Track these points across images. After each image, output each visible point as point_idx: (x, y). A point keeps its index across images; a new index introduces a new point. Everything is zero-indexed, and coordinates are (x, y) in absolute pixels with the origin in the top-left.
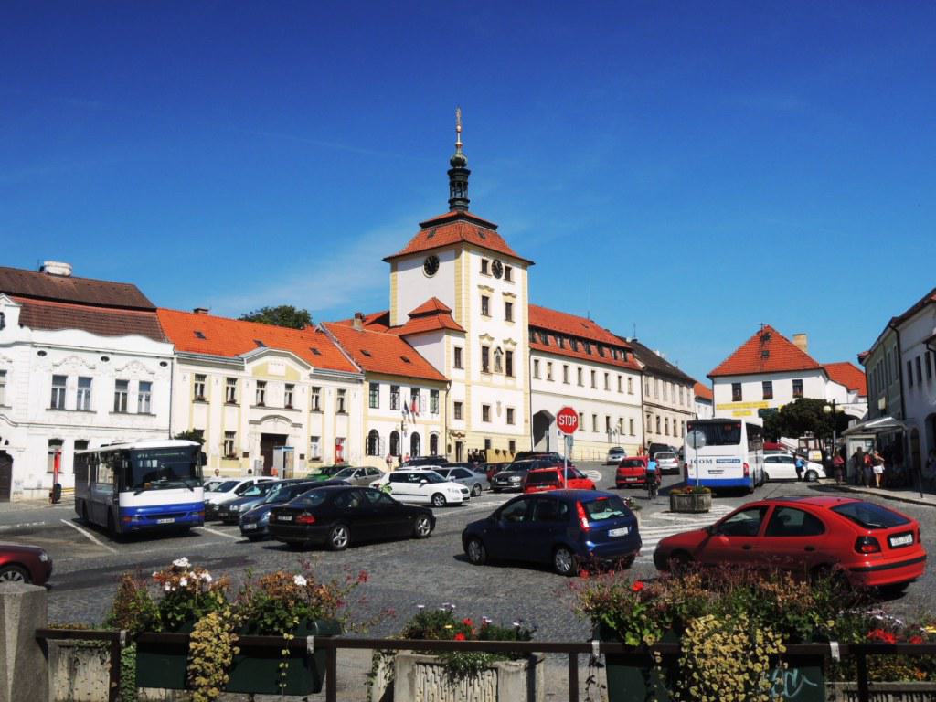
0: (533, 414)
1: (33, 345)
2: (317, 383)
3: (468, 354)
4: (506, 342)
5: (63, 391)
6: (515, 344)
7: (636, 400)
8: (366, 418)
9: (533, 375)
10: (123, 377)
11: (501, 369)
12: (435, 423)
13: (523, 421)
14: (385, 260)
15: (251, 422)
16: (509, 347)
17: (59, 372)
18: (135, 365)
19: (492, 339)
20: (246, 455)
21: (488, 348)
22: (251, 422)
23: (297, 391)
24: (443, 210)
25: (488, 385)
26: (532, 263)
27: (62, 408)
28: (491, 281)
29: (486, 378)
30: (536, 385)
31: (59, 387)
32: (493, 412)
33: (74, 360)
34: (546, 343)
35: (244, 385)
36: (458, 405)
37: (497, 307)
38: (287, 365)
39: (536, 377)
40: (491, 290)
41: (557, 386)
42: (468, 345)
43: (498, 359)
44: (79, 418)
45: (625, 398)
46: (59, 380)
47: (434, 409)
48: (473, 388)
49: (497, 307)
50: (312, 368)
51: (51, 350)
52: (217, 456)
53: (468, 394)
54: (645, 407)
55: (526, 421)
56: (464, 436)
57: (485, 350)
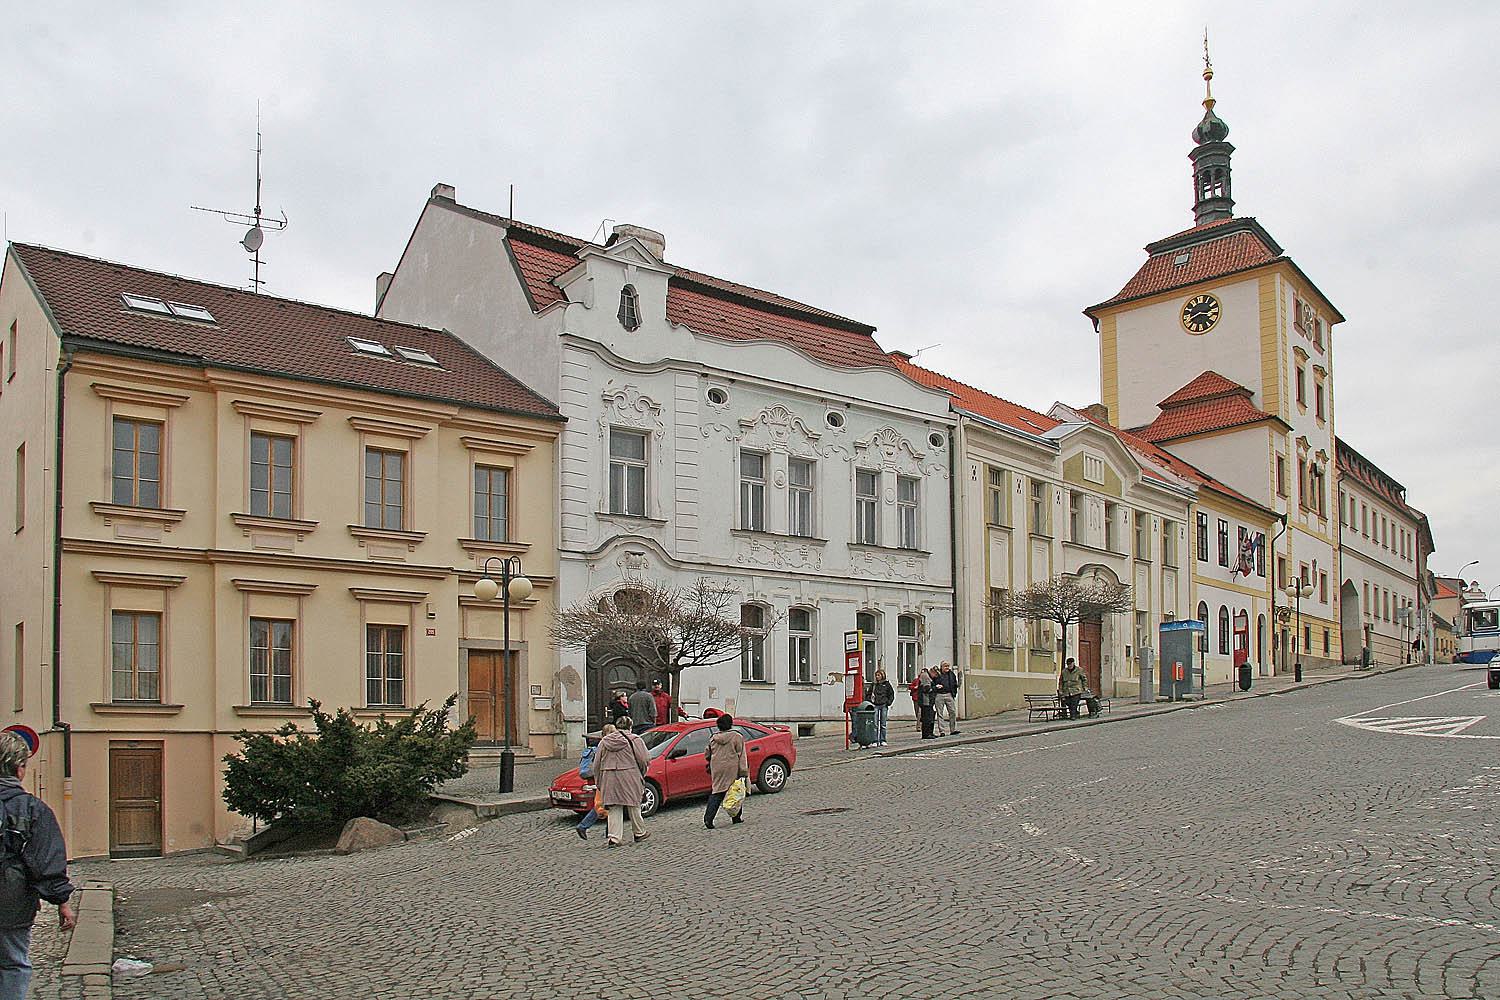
2: (1143, 506)
10: (870, 460)
17: (753, 441)
23: (1120, 513)
44: (793, 557)
46: (754, 461)
51: (734, 386)
57: (1302, 463)
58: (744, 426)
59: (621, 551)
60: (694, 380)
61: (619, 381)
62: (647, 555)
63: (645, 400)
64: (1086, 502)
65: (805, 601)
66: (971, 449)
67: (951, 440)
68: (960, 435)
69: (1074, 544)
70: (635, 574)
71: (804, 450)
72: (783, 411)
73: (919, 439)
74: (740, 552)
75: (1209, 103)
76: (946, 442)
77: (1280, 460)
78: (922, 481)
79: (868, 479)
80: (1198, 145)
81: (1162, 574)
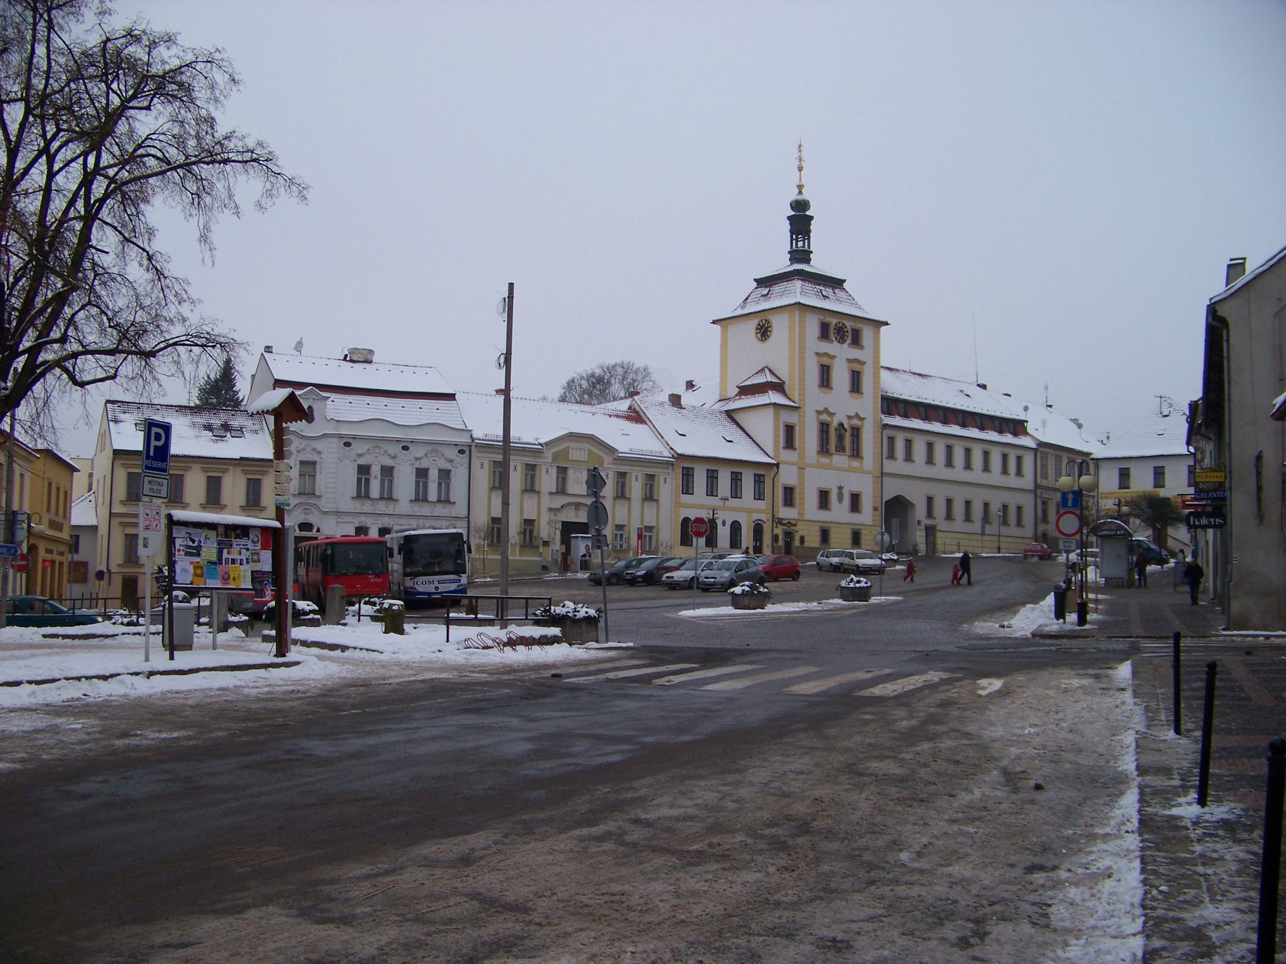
0: (886, 498)
1: (340, 436)
2: (623, 469)
3: (802, 432)
4: (849, 417)
5: (367, 481)
6: (862, 419)
7: (1027, 481)
8: (678, 505)
9: (885, 455)
12: (758, 511)
13: (872, 509)
14: (714, 322)
16: (855, 422)
17: (363, 461)
18: (434, 454)
19: (832, 415)
20: (546, 544)
21: (828, 425)
22: (550, 510)
24: (782, 263)
25: (829, 467)
26: (886, 324)
27: (367, 497)
28: (833, 348)
29: (824, 460)
30: (890, 466)
31: (363, 477)
33: (377, 450)
35: (544, 471)
36: (789, 492)
37: (841, 377)
38: (589, 450)
39: (891, 456)
40: (833, 357)
41: (919, 466)
42: (802, 423)
43: (840, 438)
44: (382, 507)
45: (1012, 481)
46: (364, 470)
48: (807, 470)
49: (841, 377)
51: (356, 440)
52: (516, 544)
53: (801, 477)
54: (1039, 492)
55: (875, 509)
56: (795, 525)
58: (360, 455)
59: (301, 508)
60: (335, 440)
61: (304, 443)
62: (313, 509)
63: (314, 450)
64: (571, 473)
65: (386, 525)
66: (480, 455)
67: (470, 451)
68: (473, 449)
69: (561, 490)
70: (307, 517)
71: (389, 462)
72: (379, 448)
73: (452, 453)
74: (357, 506)
75: (800, 187)
76: (467, 452)
77: (790, 429)
78: (453, 473)
79: (422, 473)
80: (793, 213)
81: (643, 506)
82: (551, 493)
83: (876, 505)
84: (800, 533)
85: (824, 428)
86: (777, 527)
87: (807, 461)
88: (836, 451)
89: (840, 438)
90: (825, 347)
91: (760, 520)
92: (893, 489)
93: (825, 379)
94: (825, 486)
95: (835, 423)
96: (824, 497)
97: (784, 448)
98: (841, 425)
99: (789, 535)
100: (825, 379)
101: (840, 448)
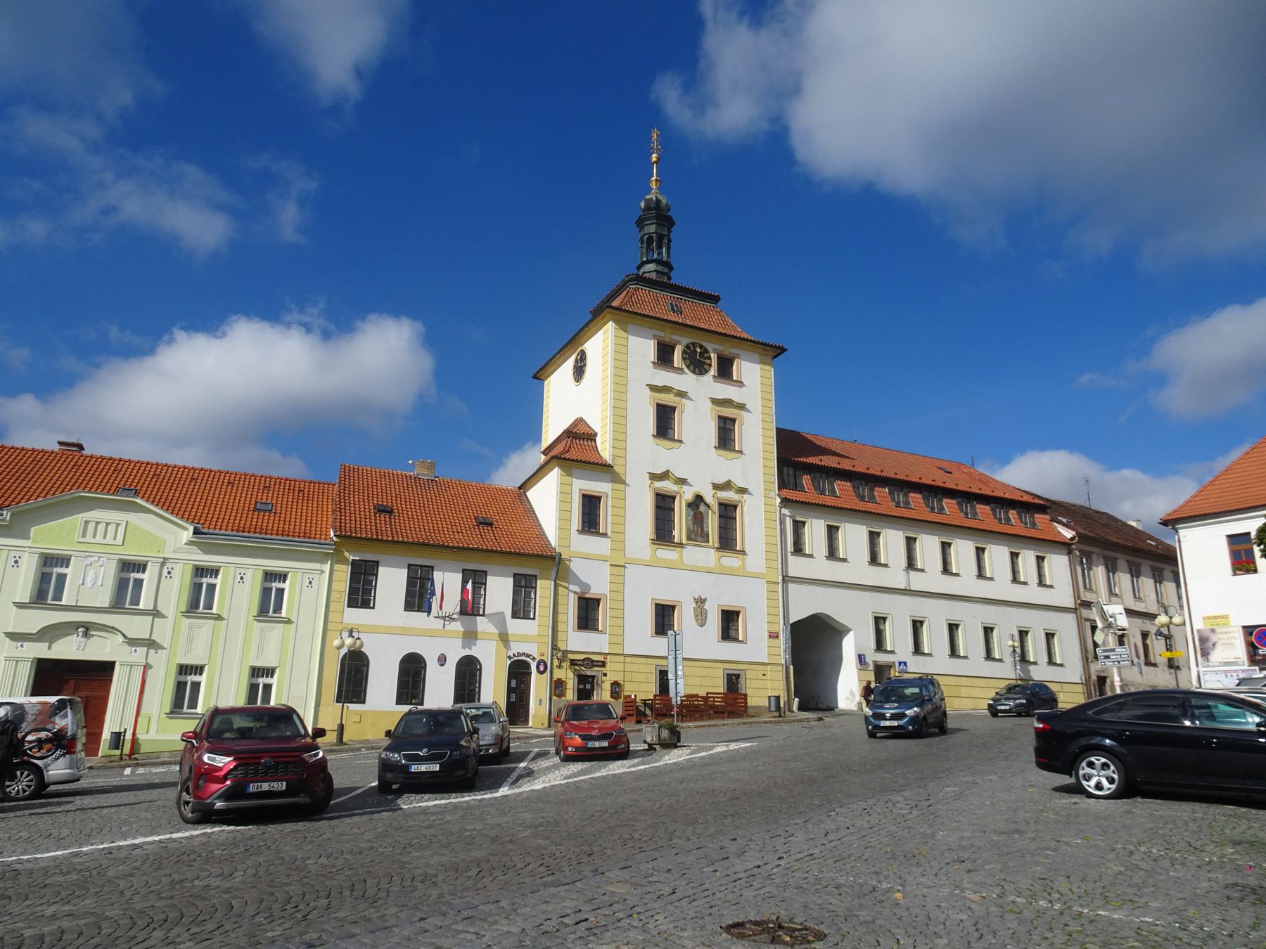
4: (717, 487)
9: (790, 547)
11: (705, 537)
13: (767, 636)
15: (13, 636)
26: (782, 350)
29: (666, 553)
32: (684, 619)
34: (872, 499)
39: (798, 549)
43: (698, 519)
47: (521, 609)
48: (631, 571)
50: (191, 528)
53: (618, 585)
55: (774, 635)
82: (20, 605)
83: (774, 629)
84: (611, 677)
85: (664, 504)
86: (560, 667)
87: (631, 553)
88: (689, 538)
89: (698, 519)
90: (664, 377)
91: (528, 656)
92: (804, 605)
93: (665, 421)
94: (666, 597)
95: (688, 494)
96: (664, 617)
97: (580, 532)
98: (699, 498)
99: (586, 685)
100: (665, 421)
101: (698, 534)
